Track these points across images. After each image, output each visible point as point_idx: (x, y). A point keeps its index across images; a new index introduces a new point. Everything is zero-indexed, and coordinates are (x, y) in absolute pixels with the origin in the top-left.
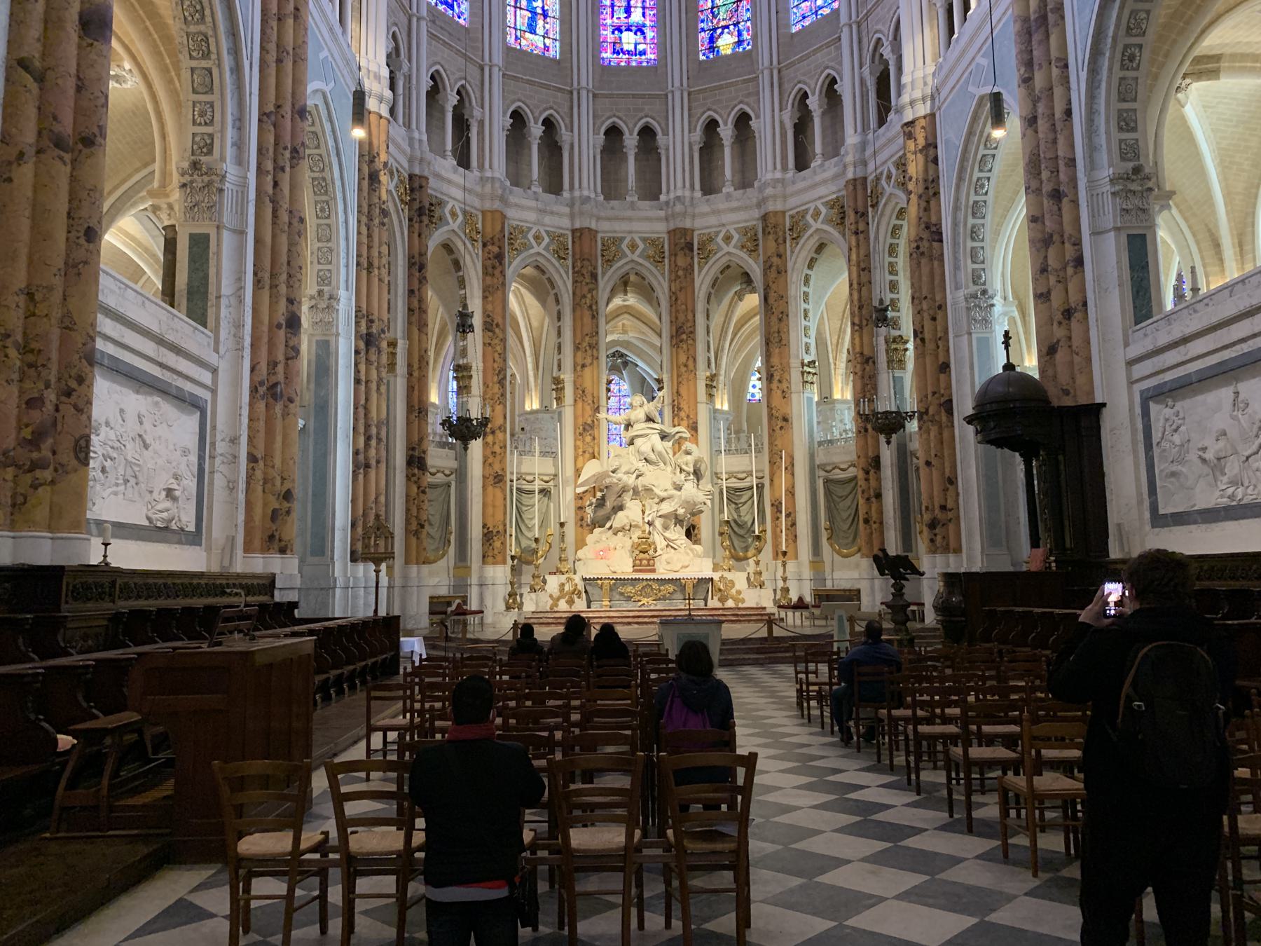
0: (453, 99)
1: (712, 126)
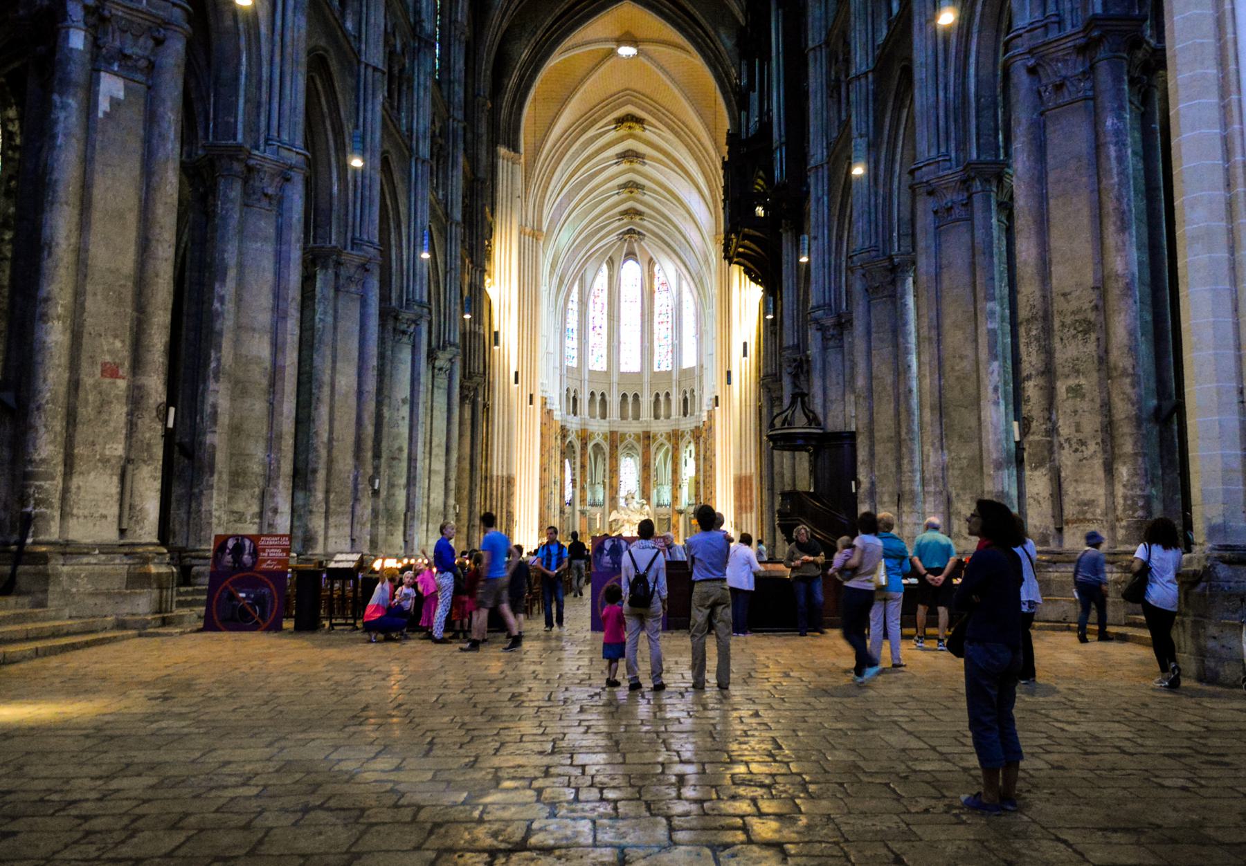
0: (572, 394)
1: (657, 395)
